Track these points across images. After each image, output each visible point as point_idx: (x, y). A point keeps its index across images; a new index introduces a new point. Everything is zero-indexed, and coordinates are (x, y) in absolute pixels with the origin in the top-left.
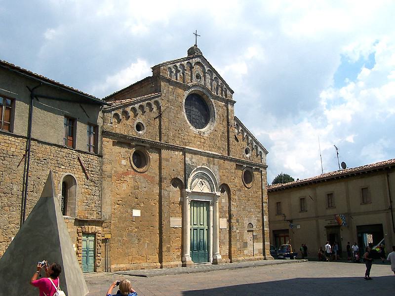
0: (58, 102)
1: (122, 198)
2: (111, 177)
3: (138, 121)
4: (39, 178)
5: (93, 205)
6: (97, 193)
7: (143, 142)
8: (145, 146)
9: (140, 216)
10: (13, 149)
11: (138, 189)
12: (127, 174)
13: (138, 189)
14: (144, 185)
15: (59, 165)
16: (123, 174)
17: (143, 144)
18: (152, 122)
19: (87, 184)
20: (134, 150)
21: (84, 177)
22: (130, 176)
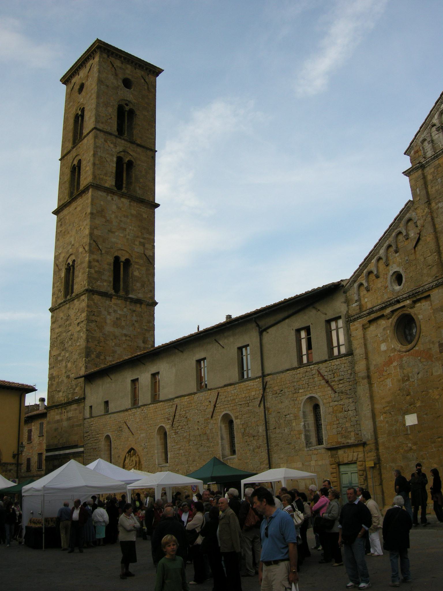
0: (287, 321)
1: (389, 403)
2: (369, 377)
3: (391, 273)
4: (279, 412)
5: (348, 425)
6: (352, 407)
7: (398, 302)
8: (404, 307)
9: (416, 423)
10: (253, 393)
11: (408, 380)
12: (390, 361)
13: (408, 380)
14: (416, 370)
15: (296, 391)
16: (384, 366)
17: (402, 304)
18: (412, 257)
19: (335, 399)
20: (393, 320)
21: (330, 392)
22: (395, 364)
